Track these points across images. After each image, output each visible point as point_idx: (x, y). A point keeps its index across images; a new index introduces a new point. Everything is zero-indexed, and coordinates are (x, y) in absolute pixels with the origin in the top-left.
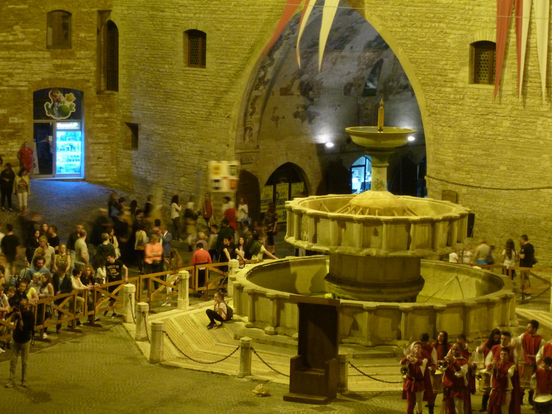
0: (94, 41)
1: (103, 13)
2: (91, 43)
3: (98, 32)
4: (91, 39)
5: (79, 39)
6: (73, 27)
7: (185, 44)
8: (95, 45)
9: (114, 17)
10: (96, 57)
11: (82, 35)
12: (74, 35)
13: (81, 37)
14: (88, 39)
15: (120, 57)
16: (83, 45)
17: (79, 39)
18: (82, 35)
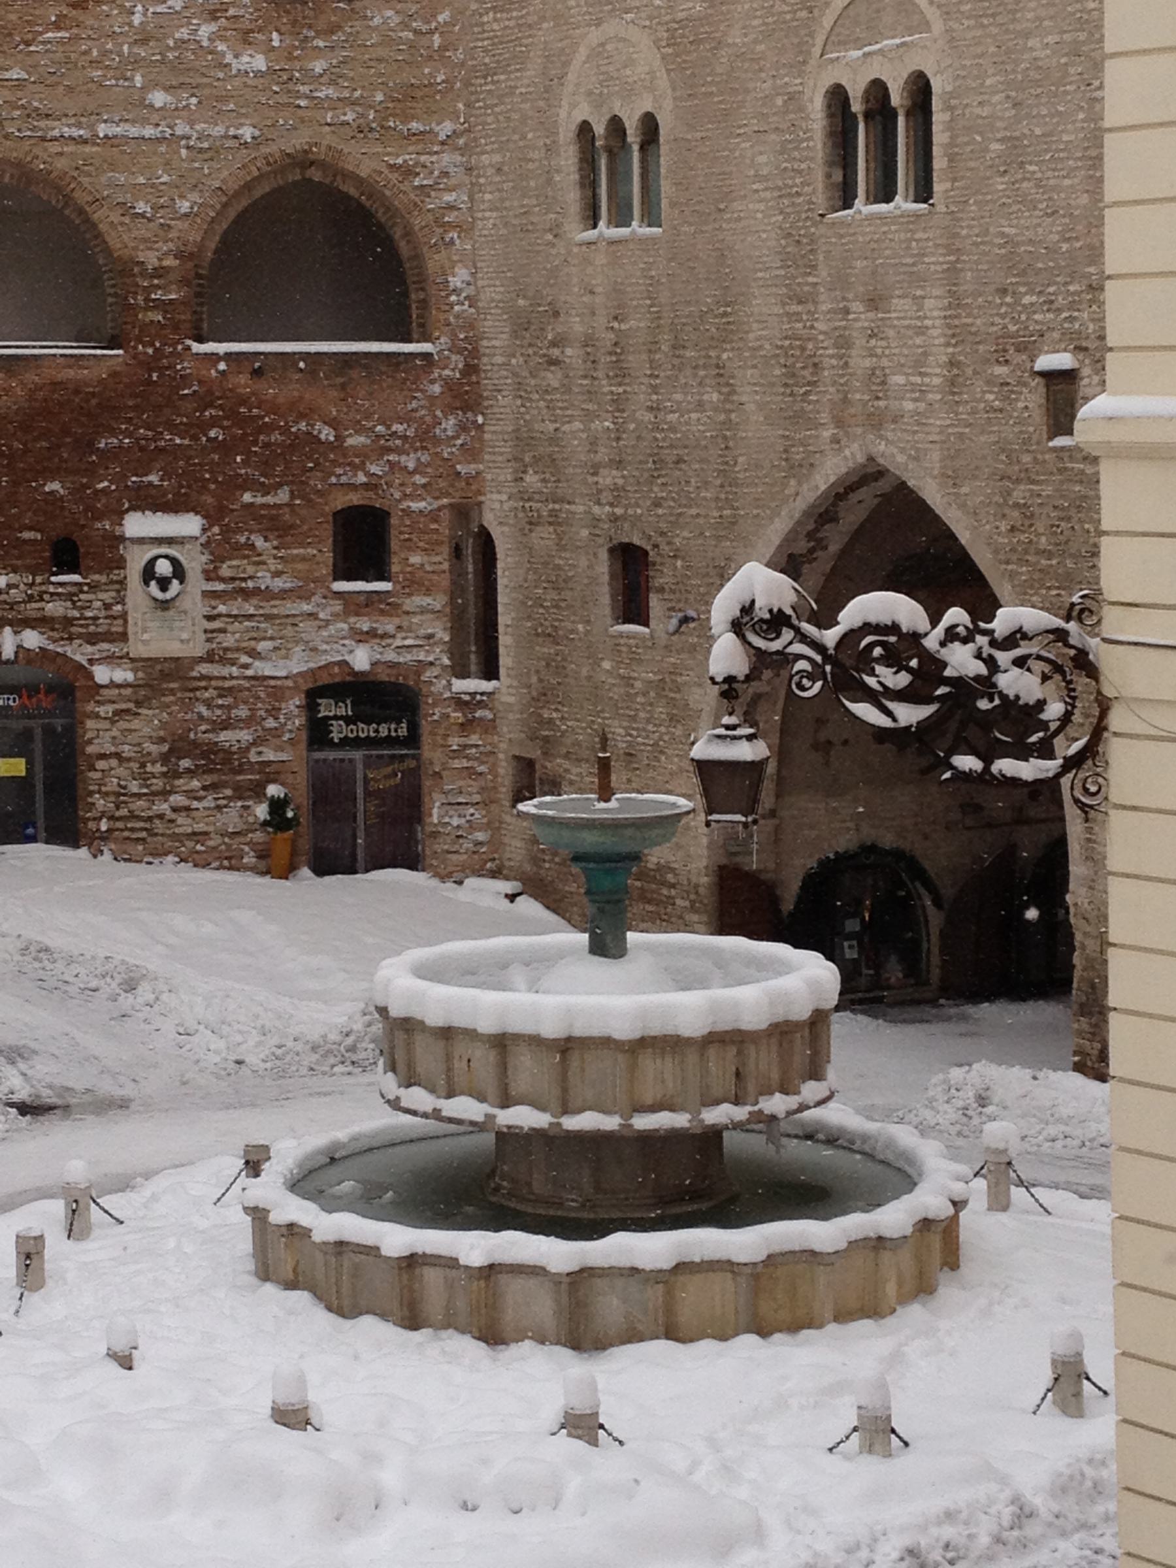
0: (444, 572)
1: (464, 512)
2: (435, 577)
3: (457, 552)
4: (436, 567)
5: (409, 569)
6: (394, 545)
7: (612, 576)
8: (445, 581)
9: (489, 520)
10: (448, 610)
11: (415, 559)
12: (395, 559)
13: (413, 565)
14: (428, 568)
15: (500, 609)
16: (415, 583)
17: (409, 569)
18: (415, 559)
